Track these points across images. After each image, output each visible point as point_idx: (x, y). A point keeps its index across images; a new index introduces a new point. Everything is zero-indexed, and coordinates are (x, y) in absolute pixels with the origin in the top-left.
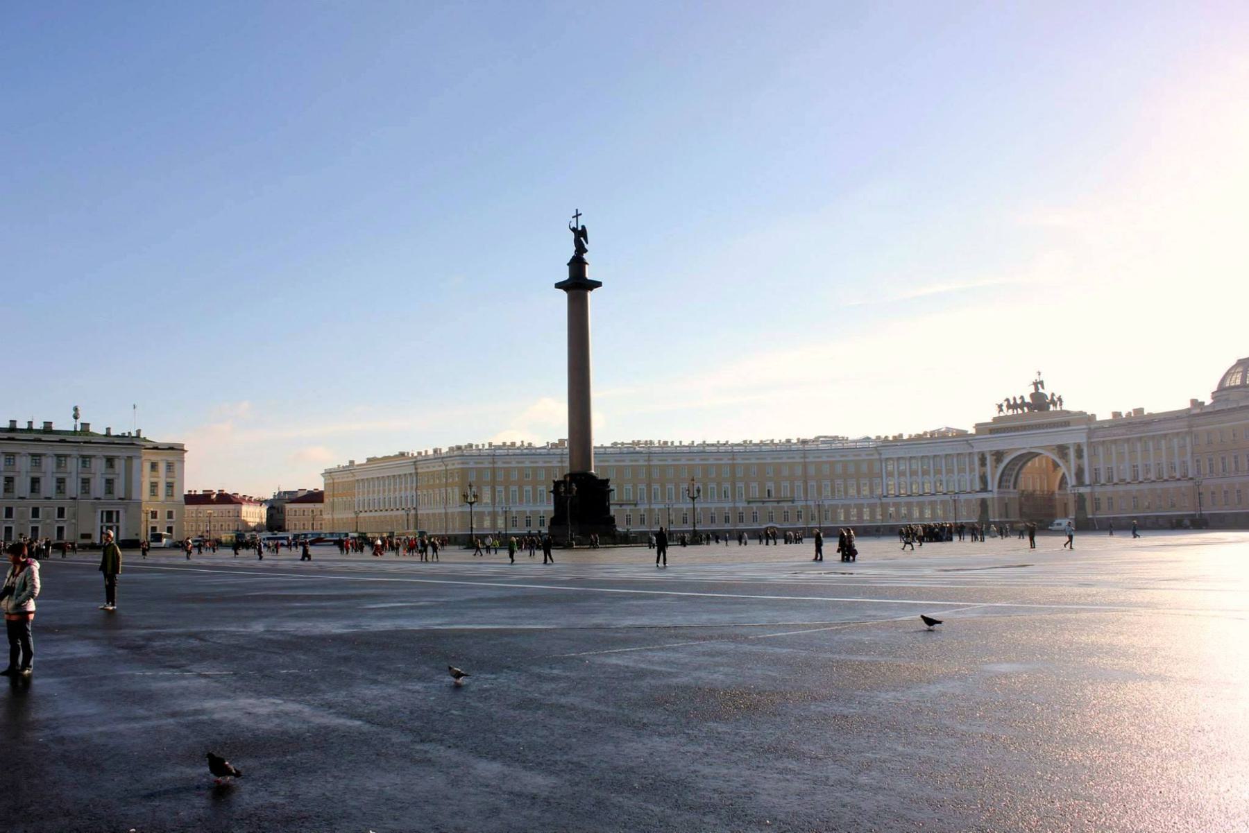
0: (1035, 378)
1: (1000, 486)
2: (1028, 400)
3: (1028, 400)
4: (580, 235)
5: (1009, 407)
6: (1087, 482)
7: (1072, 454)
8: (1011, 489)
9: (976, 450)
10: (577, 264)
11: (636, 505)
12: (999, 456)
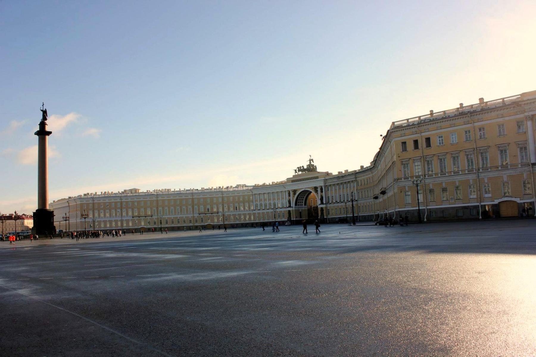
0: (309, 158)
1: (296, 205)
2: (305, 167)
3: (305, 167)
4: (45, 113)
5: (299, 171)
6: (324, 203)
7: (319, 190)
8: (303, 206)
9: (286, 190)
10: (43, 125)
11: (152, 216)
12: (295, 192)
